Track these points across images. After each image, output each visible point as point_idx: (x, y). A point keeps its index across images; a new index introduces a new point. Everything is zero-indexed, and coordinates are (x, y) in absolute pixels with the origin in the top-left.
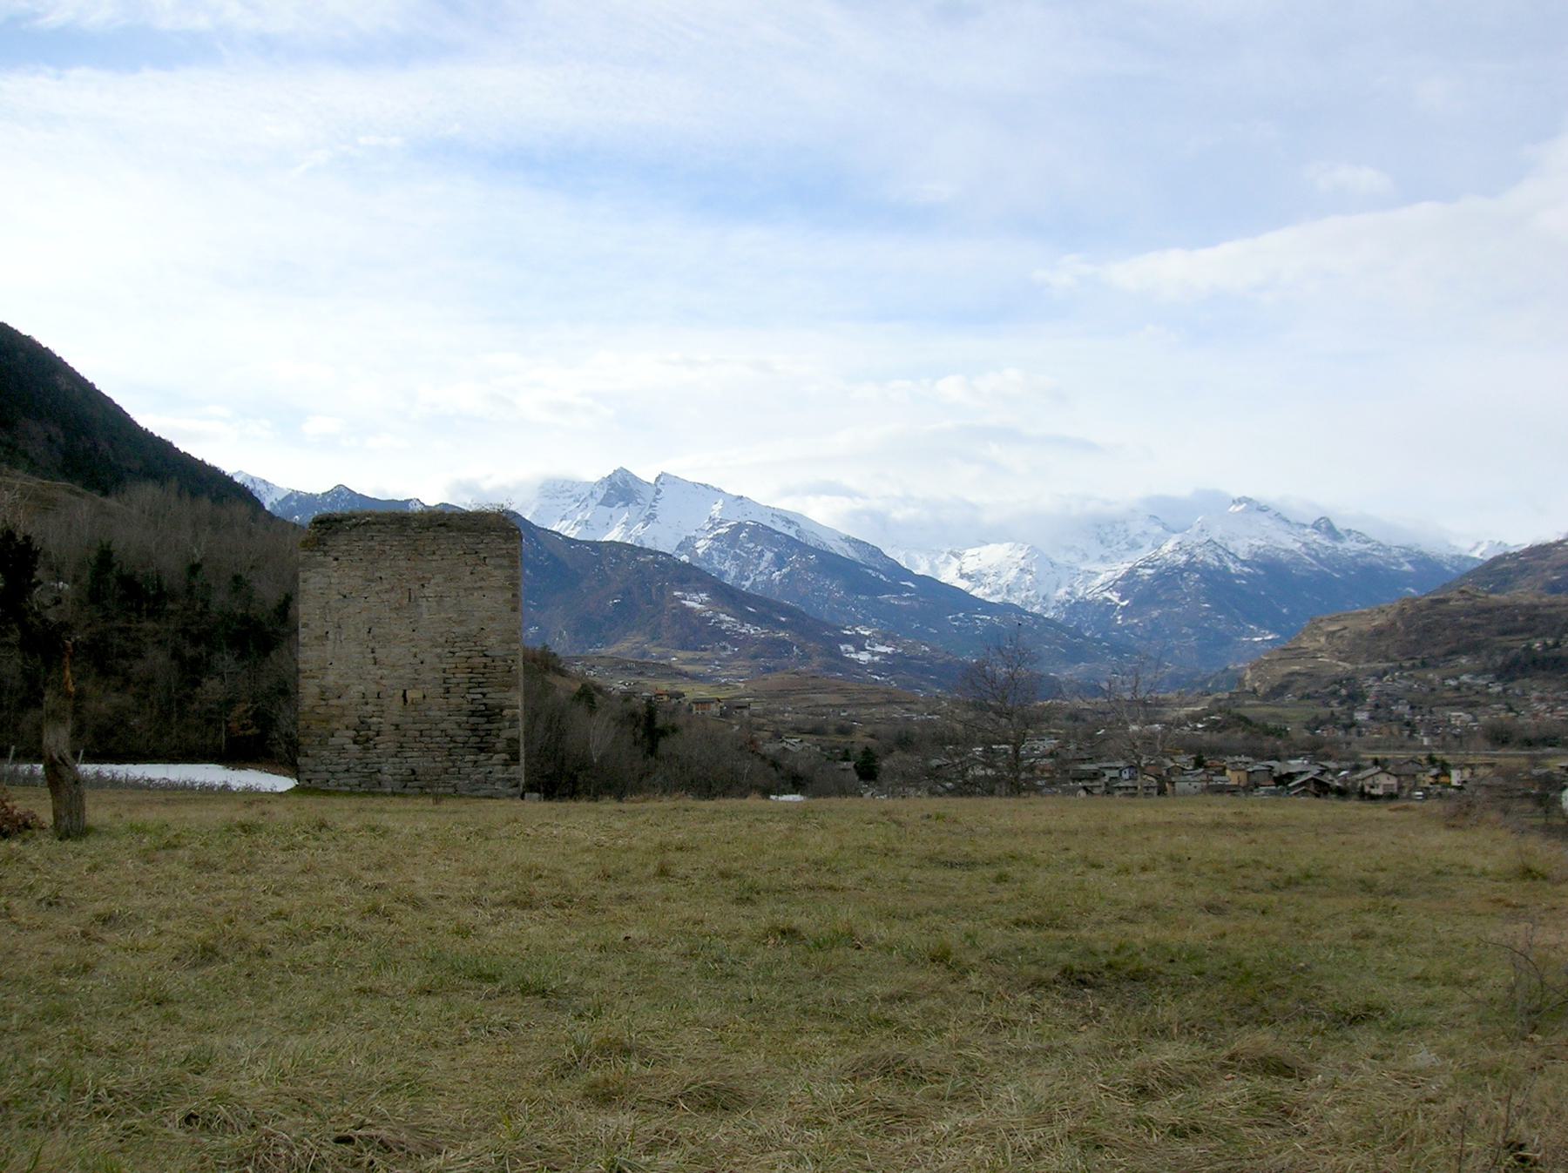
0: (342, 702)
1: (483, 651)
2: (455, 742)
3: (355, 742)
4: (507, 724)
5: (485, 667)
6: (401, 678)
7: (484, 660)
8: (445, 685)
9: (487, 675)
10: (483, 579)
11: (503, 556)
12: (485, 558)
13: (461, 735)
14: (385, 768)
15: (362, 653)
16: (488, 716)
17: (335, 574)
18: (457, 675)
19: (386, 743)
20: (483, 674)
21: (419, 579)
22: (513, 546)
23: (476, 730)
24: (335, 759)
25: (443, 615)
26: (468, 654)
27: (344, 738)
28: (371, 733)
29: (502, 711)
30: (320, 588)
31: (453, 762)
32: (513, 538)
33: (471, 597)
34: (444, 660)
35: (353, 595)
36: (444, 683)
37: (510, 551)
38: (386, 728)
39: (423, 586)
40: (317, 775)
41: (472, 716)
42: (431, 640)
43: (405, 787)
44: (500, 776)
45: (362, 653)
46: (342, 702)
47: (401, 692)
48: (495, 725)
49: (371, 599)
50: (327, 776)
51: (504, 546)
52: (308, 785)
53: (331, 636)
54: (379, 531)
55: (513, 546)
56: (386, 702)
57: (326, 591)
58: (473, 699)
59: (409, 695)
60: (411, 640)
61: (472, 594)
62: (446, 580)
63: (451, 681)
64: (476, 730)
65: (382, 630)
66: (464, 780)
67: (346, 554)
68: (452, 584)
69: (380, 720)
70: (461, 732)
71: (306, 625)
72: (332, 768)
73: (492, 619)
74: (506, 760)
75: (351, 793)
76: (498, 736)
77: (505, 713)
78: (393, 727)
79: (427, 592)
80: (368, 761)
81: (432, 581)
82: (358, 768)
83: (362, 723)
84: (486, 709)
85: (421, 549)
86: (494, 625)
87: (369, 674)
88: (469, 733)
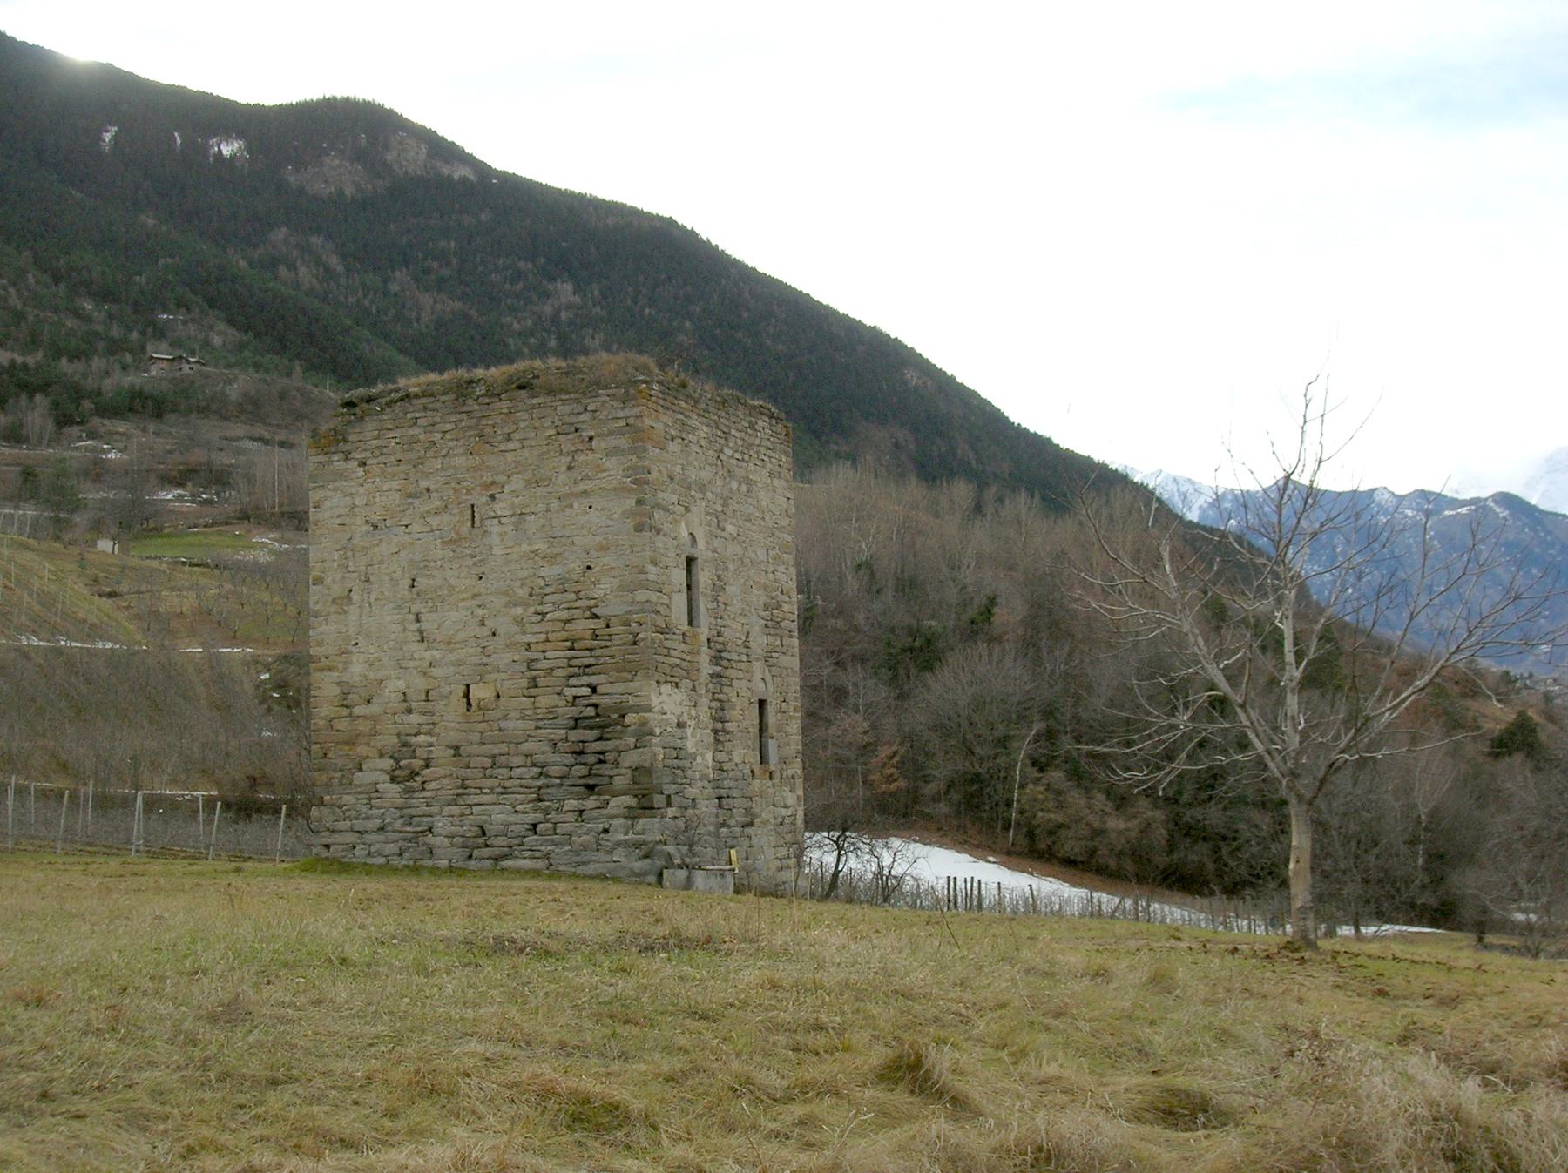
0: (374, 709)
1: (589, 608)
2: (547, 776)
3: (393, 780)
4: (632, 740)
5: (595, 636)
6: (459, 663)
7: (592, 624)
8: (529, 674)
9: (598, 652)
10: (587, 478)
11: (619, 433)
12: (591, 438)
13: (558, 762)
14: (440, 824)
15: (402, 622)
16: (602, 727)
17: (361, 490)
18: (548, 655)
19: (440, 780)
20: (591, 650)
21: (487, 486)
22: (636, 411)
23: (581, 753)
24: (364, 809)
25: (525, 548)
26: (565, 615)
27: (376, 772)
28: (417, 763)
29: (623, 716)
30: (340, 516)
31: (546, 812)
32: (635, 398)
33: (568, 511)
34: (529, 628)
35: (388, 523)
36: (529, 669)
37: (632, 421)
38: (437, 752)
39: (492, 497)
40: (337, 838)
41: (575, 727)
42: (506, 593)
43: (470, 857)
44: (622, 837)
45: (402, 622)
46: (374, 709)
47: (464, 688)
48: (610, 745)
49: (414, 528)
50: (352, 838)
51: (621, 414)
52: (325, 853)
53: (355, 597)
54: (425, 409)
55: (636, 411)
56: (439, 706)
57: (347, 521)
58: (576, 697)
59: (475, 693)
60: (475, 596)
61: (571, 506)
62: (528, 483)
63: (539, 666)
64: (581, 753)
65: (431, 582)
66: (562, 844)
67: (377, 453)
68: (539, 491)
69: (429, 739)
70: (556, 758)
71: (319, 581)
72: (359, 825)
73: (604, 548)
74: (630, 808)
75: (387, 869)
76: (616, 764)
77: (627, 720)
78: (452, 752)
79: (500, 508)
80: (413, 812)
81: (507, 489)
82: (398, 825)
83: (404, 745)
84: (598, 715)
85: (488, 430)
86: (608, 559)
87: (412, 659)
88: (570, 759)
